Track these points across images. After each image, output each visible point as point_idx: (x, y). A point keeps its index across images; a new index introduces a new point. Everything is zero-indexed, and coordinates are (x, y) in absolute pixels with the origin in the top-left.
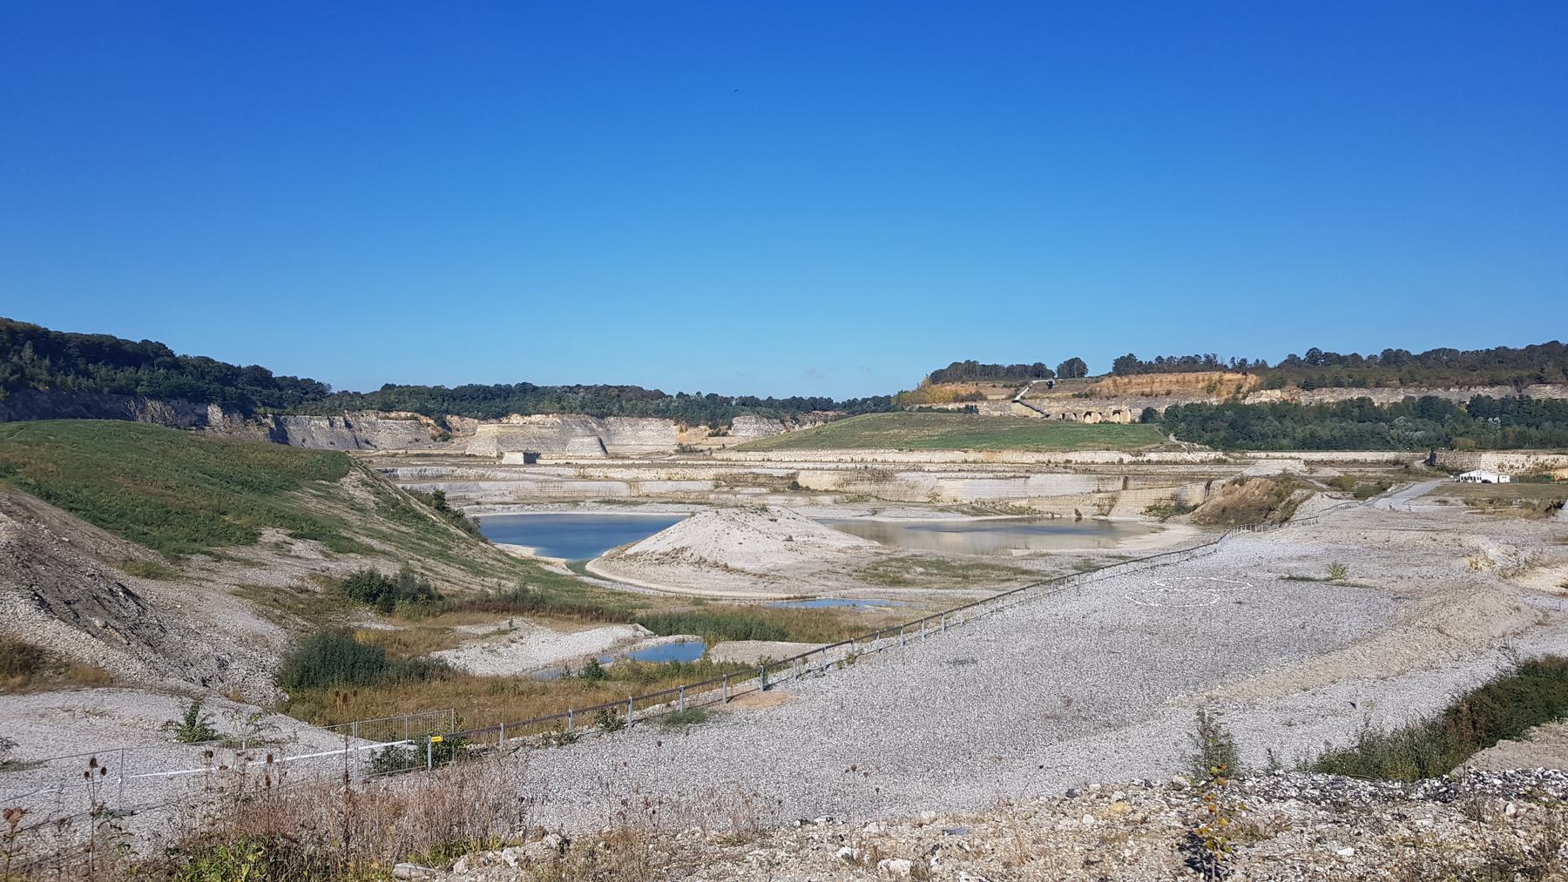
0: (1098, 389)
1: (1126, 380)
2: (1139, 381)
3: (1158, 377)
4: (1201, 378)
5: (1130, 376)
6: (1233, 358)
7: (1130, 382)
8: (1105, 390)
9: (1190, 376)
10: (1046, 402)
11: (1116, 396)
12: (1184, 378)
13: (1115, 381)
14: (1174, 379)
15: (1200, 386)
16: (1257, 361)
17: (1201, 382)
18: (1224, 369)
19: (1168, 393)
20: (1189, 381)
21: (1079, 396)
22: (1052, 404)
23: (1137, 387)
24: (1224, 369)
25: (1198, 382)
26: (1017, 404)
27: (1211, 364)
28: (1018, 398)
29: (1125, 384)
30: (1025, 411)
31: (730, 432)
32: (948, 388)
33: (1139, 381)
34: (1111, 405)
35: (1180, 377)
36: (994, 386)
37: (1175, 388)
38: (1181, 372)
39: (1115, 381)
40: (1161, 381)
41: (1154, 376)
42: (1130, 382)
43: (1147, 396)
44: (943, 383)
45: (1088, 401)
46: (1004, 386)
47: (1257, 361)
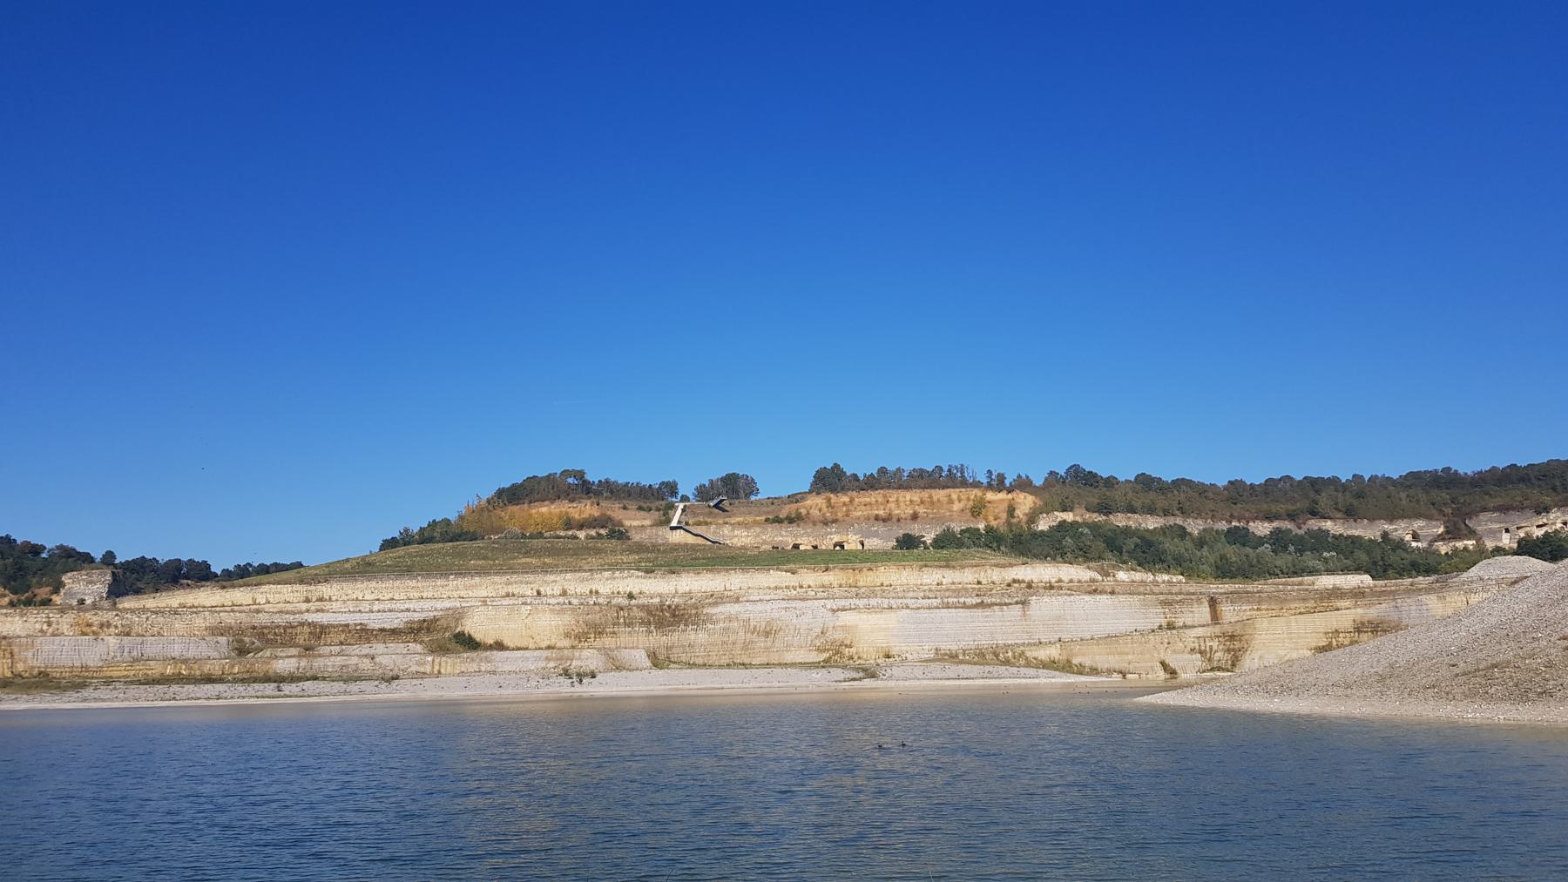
0: (803, 511)
1: (846, 499)
2: (863, 500)
3: (894, 495)
4: (954, 497)
5: (850, 493)
6: (990, 472)
7: (852, 501)
8: (815, 512)
9: (939, 494)
10: (726, 530)
11: (835, 521)
12: (931, 497)
13: (829, 500)
14: (916, 498)
15: (957, 507)
16: (1019, 476)
17: (957, 503)
18: (976, 485)
19: (915, 517)
20: (939, 500)
21: (778, 521)
22: (736, 532)
23: (864, 508)
24: (976, 485)
25: (951, 501)
26: (678, 531)
27: (954, 479)
28: (674, 523)
29: (844, 504)
30: (691, 539)
31: (57, 599)
32: (544, 510)
33: (863, 500)
34: (831, 534)
35: (925, 494)
36: (625, 508)
37: (921, 510)
38: (925, 488)
39: (829, 500)
40: (897, 501)
41: (886, 492)
42: (852, 501)
43: (884, 520)
44: (530, 502)
45: (793, 528)
46: (640, 508)
47: (1019, 476)
